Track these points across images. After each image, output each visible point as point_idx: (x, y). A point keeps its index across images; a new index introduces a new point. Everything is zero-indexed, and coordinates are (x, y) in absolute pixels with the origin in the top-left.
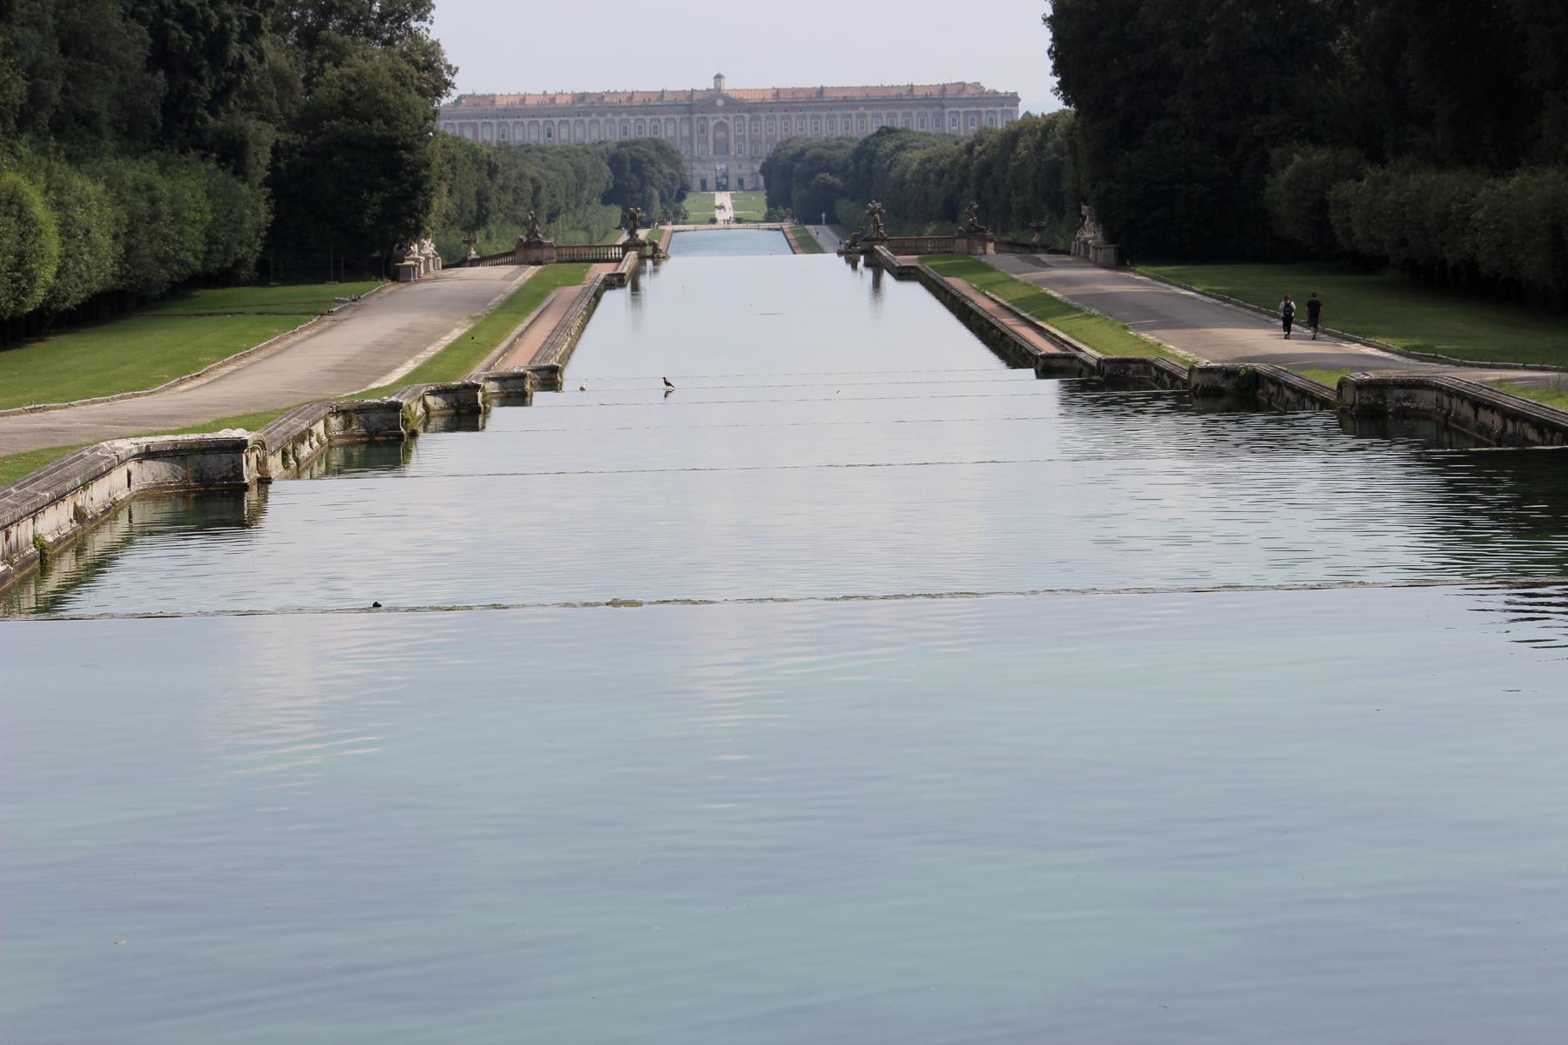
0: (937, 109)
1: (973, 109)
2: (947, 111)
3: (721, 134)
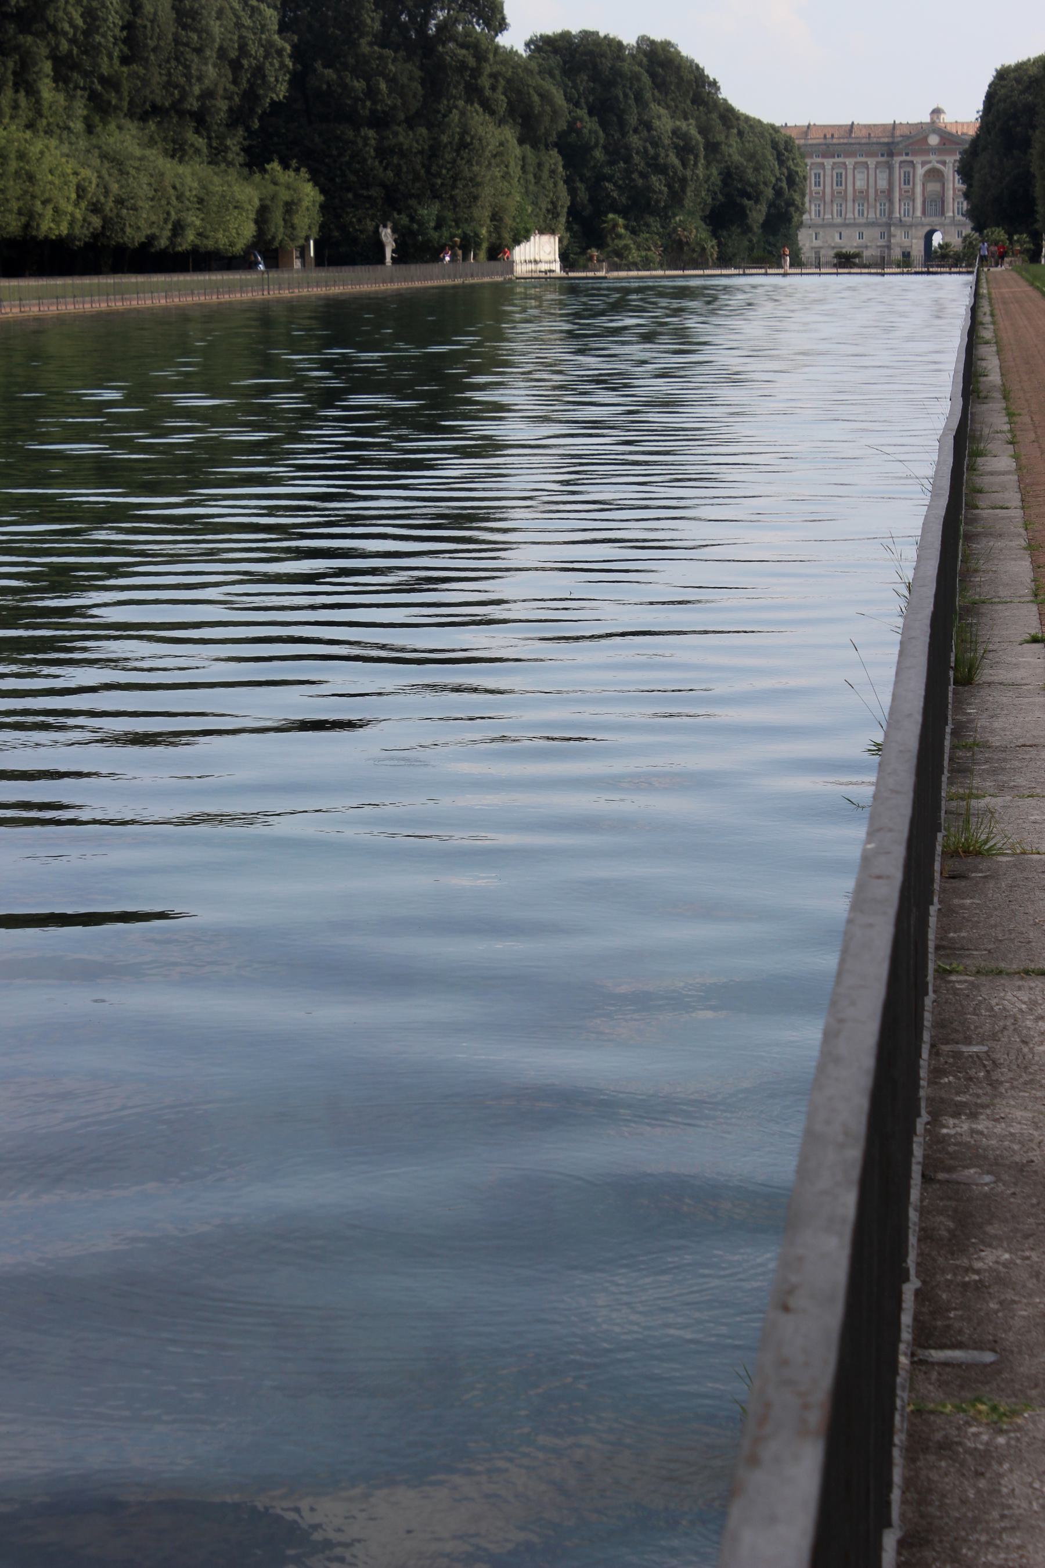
3: (933, 187)
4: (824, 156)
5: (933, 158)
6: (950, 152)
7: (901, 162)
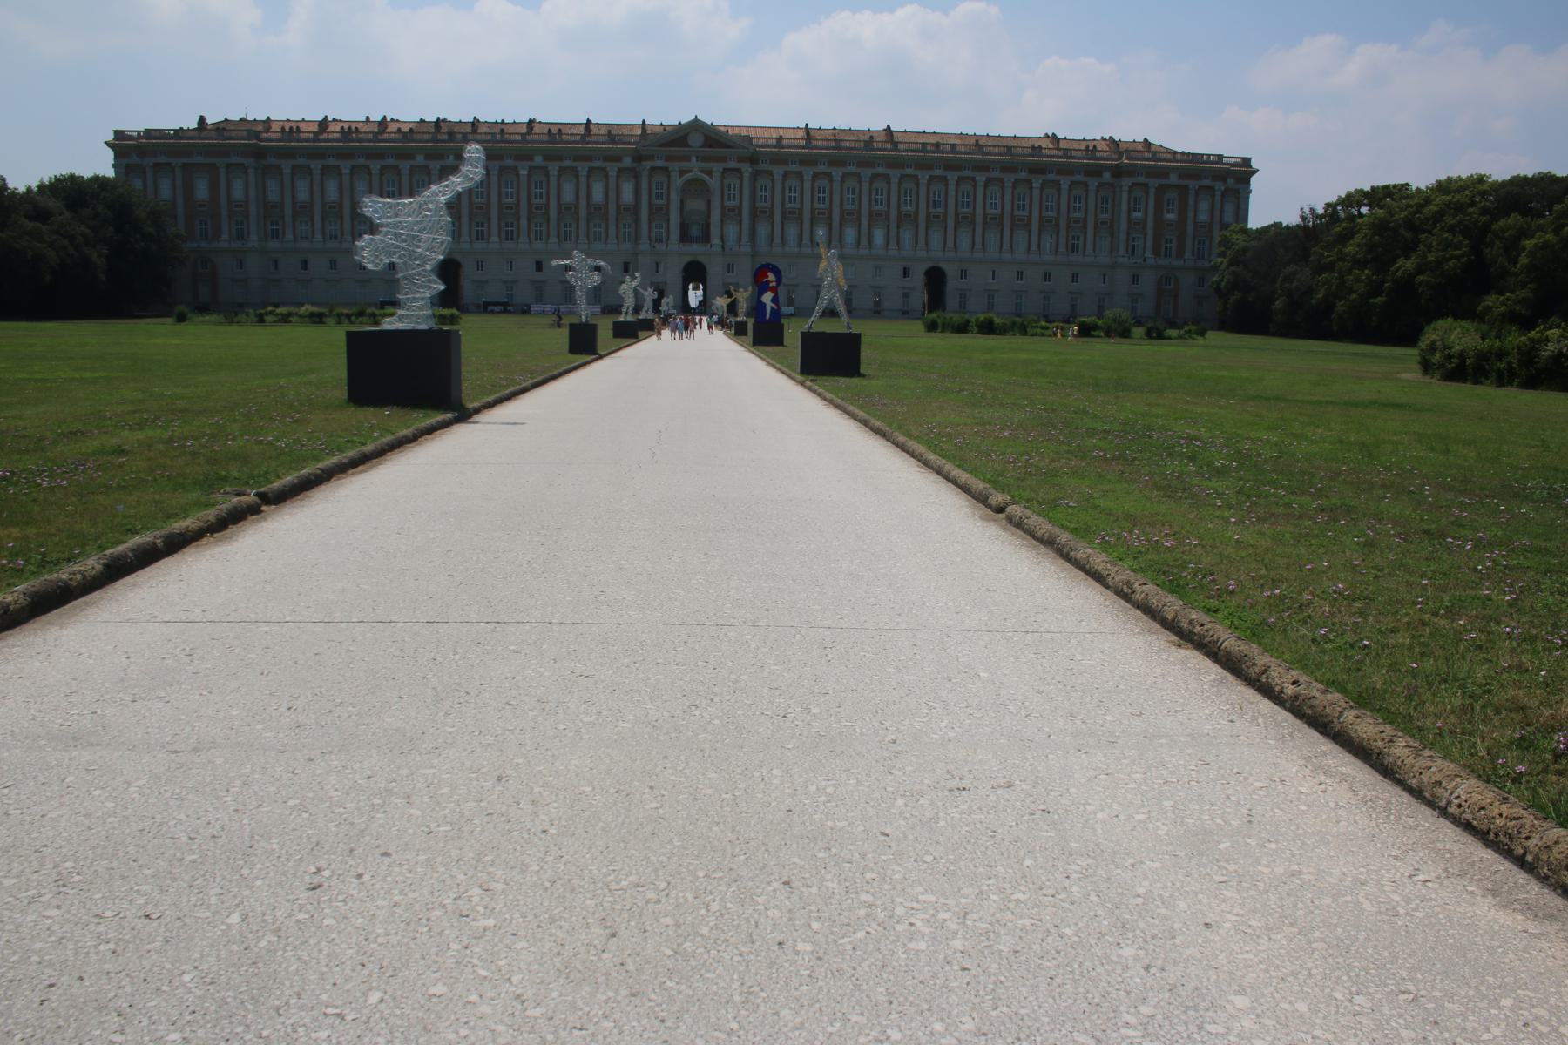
1: (1173, 179)
3: (696, 204)
7: (653, 169)
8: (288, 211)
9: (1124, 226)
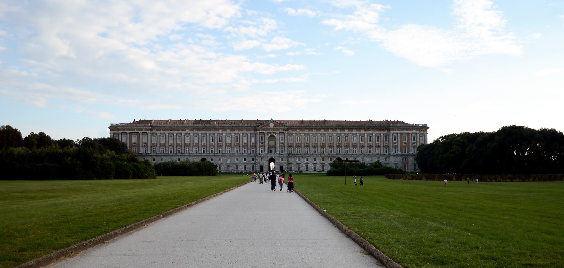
0: (386, 131)
1: (405, 132)
2: (391, 132)
3: (272, 142)
4: (231, 131)
5: (271, 131)
6: (279, 130)
8: (159, 145)
9: (392, 144)
